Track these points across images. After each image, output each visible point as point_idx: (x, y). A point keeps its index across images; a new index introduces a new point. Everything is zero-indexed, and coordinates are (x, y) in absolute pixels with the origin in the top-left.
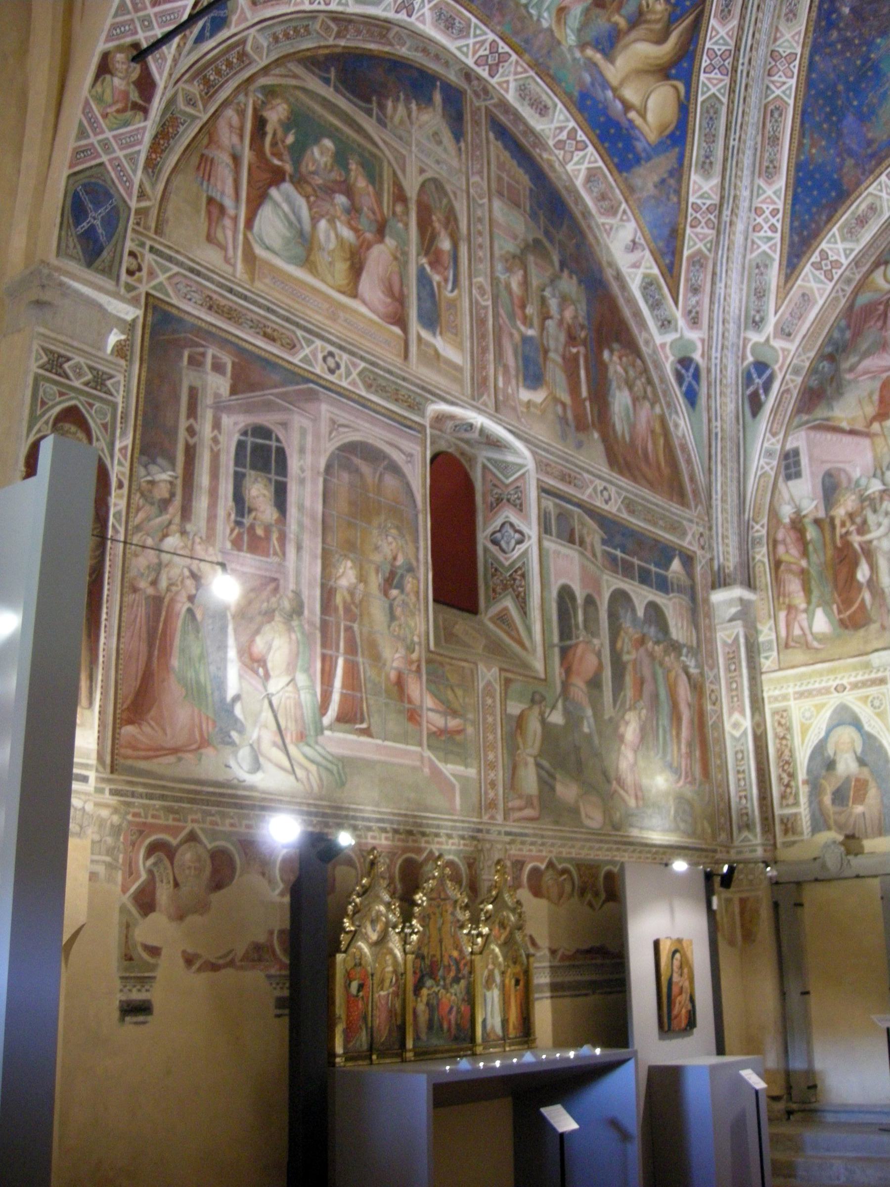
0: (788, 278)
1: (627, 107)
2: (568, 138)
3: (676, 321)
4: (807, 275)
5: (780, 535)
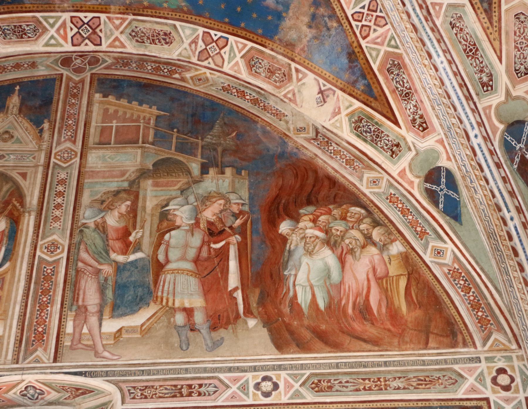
0: (488, 12)
2: (206, 45)
3: (405, 139)
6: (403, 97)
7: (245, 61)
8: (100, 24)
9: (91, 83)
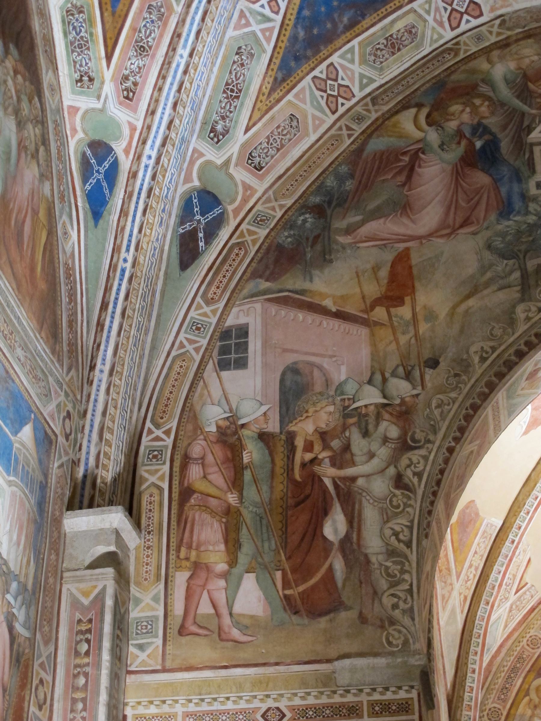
0: (277, 84)
3: (103, 83)
4: (303, 89)
5: (196, 450)
6: (137, 46)
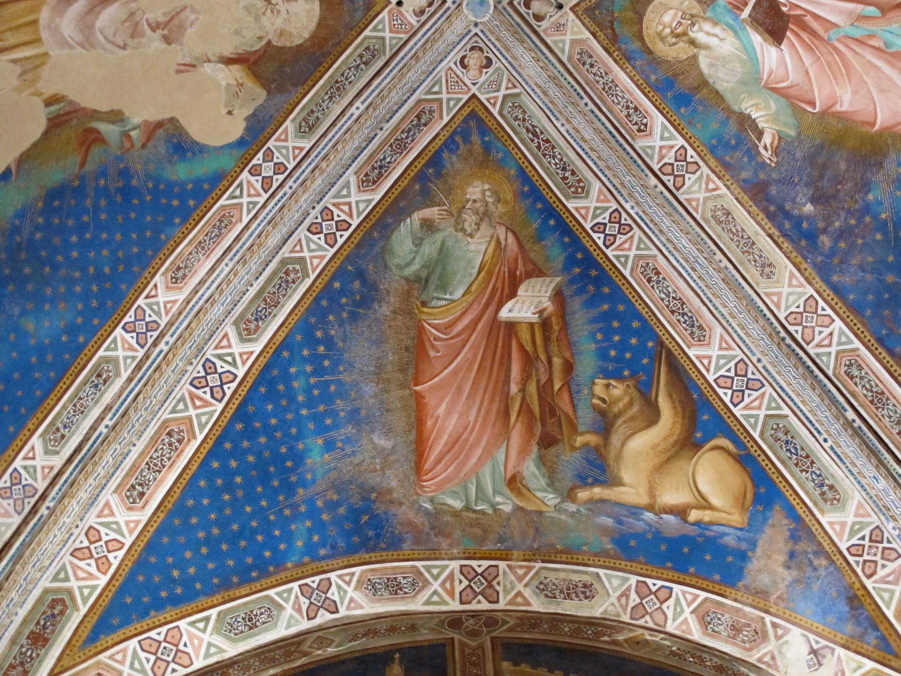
1: (681, 512)
2: (641, 599)
7: (697, 616)
8: (498, 575)
9: (493, 648)
